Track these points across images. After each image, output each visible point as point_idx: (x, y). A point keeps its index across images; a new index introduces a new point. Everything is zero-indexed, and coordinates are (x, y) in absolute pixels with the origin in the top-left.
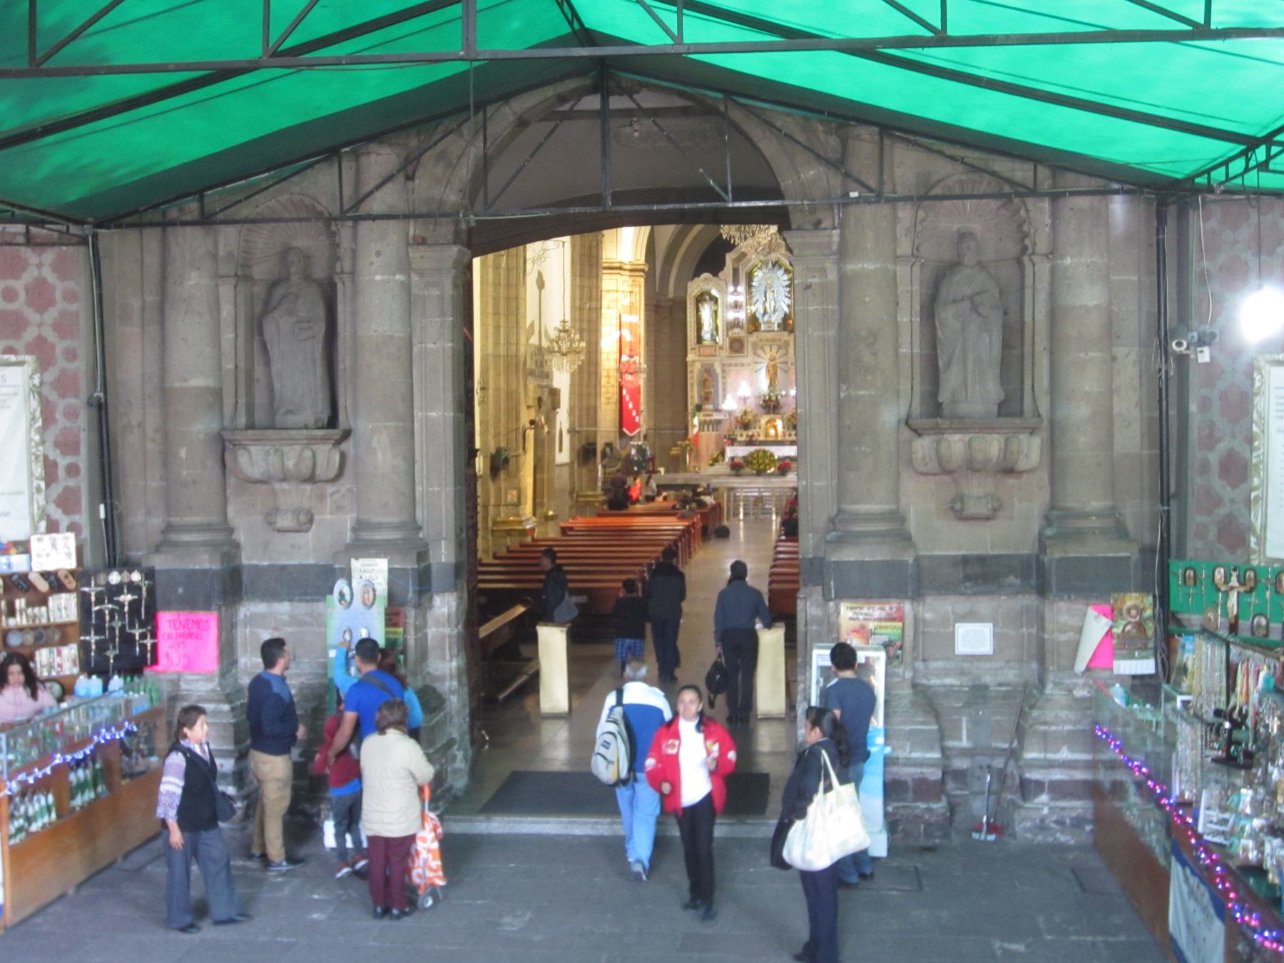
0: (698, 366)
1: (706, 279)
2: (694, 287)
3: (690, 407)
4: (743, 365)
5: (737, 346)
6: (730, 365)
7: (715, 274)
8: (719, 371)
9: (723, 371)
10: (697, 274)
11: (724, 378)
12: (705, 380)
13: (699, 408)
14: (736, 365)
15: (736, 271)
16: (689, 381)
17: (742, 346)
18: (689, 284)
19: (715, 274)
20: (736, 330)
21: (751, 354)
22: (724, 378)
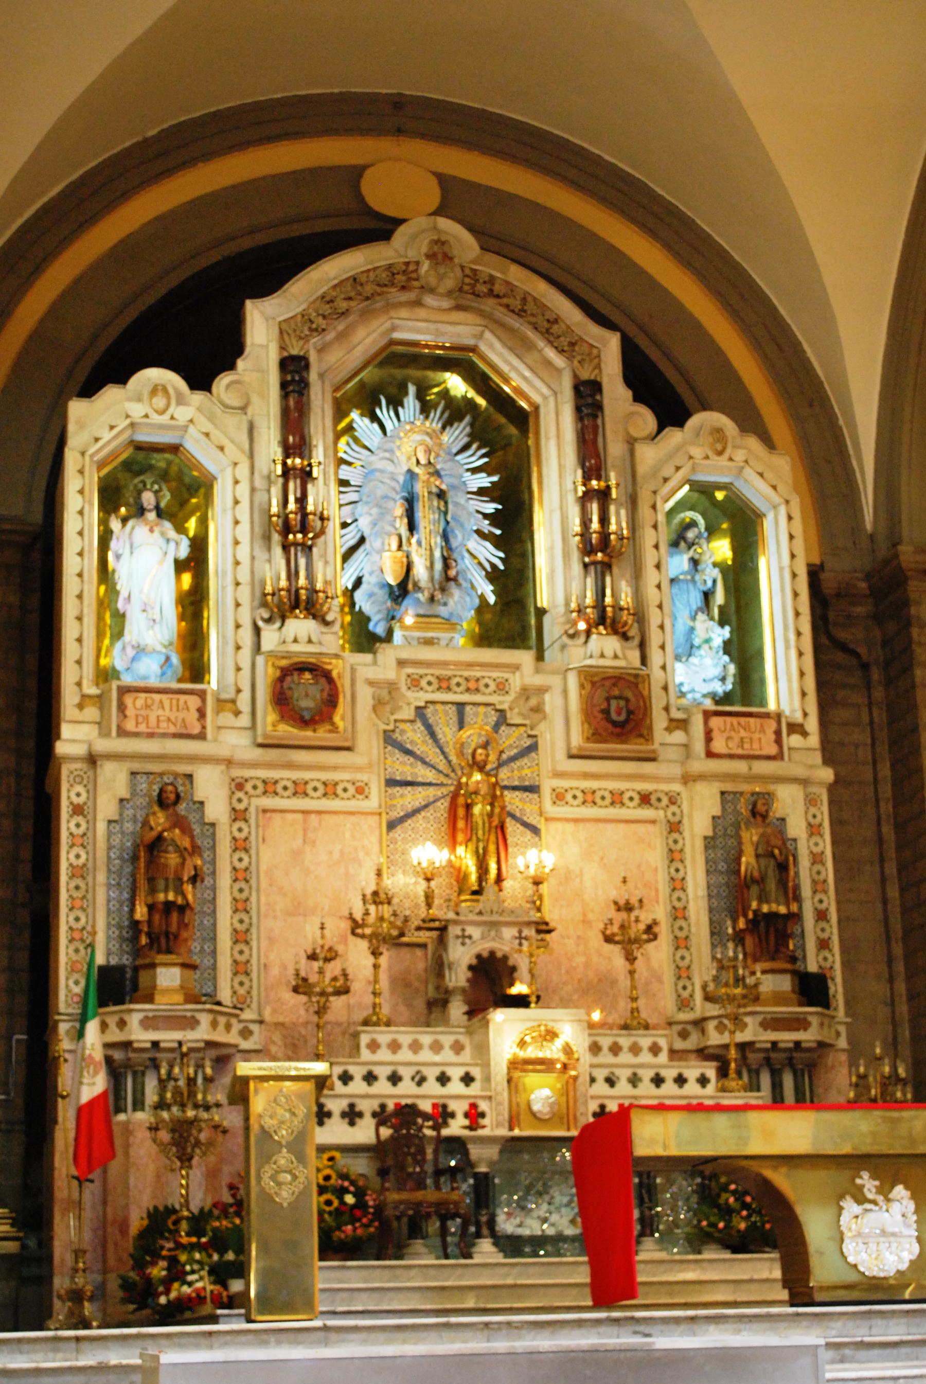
0: (114, 781)
1: (157, 389)
2: (101, 424)
3: (68, 987)
4: (330, 790)
5: (307, 693)
6: (269, 788)
7: (200, 381)
8: (217, 809)
9: (238, 815)
10: (114, 369)
11: (240, 846)
12: (152, 848)
13: (115, 987)
14: (300, 789)
15: (294, 373)
16: (67, 858)
17: (332, 701)
18: (77, 408)
19: (200, 381)
20: (300, 627)
21: (368, 744)
22: (240, 846)
